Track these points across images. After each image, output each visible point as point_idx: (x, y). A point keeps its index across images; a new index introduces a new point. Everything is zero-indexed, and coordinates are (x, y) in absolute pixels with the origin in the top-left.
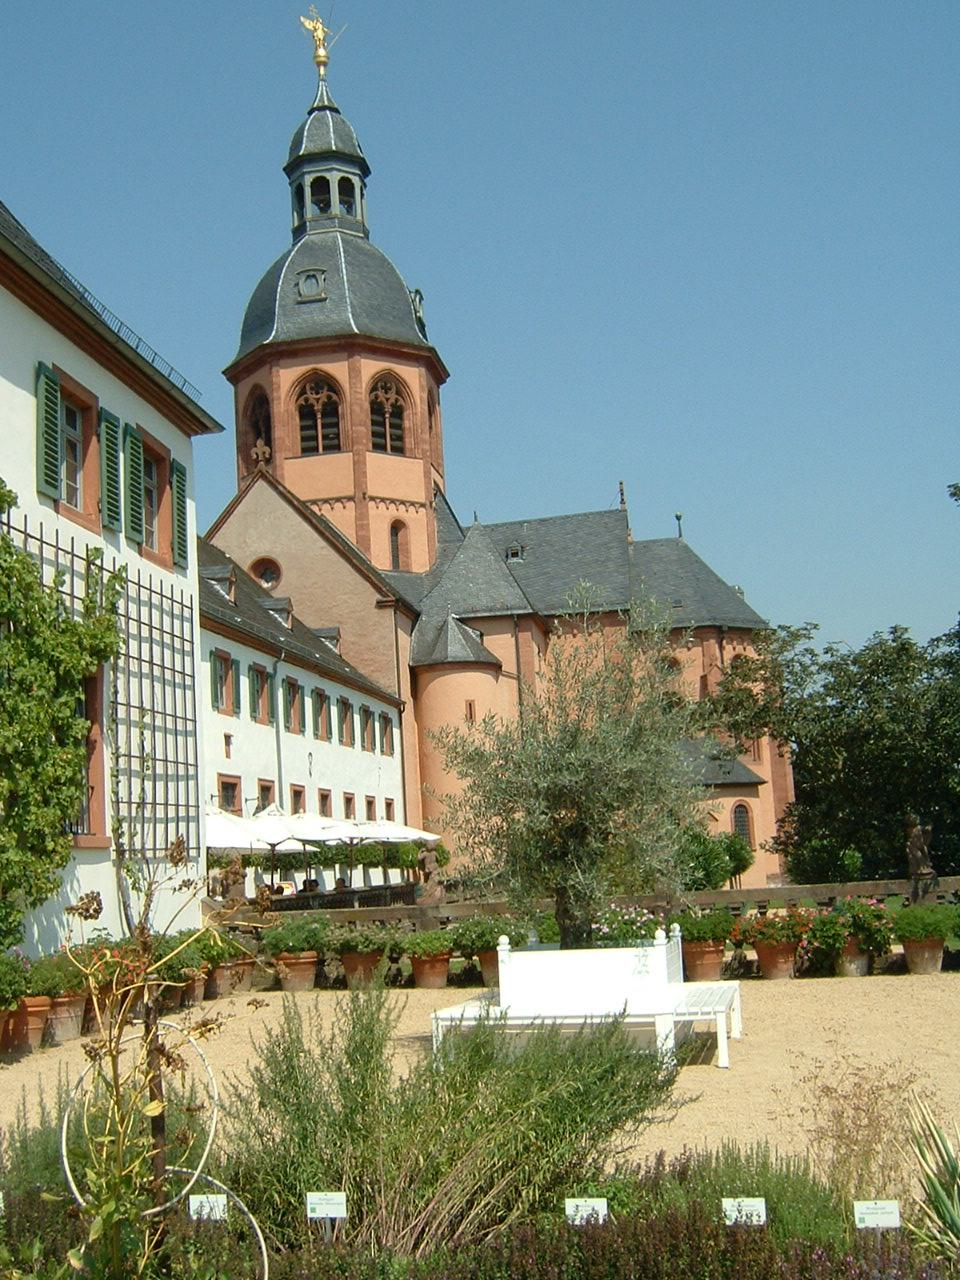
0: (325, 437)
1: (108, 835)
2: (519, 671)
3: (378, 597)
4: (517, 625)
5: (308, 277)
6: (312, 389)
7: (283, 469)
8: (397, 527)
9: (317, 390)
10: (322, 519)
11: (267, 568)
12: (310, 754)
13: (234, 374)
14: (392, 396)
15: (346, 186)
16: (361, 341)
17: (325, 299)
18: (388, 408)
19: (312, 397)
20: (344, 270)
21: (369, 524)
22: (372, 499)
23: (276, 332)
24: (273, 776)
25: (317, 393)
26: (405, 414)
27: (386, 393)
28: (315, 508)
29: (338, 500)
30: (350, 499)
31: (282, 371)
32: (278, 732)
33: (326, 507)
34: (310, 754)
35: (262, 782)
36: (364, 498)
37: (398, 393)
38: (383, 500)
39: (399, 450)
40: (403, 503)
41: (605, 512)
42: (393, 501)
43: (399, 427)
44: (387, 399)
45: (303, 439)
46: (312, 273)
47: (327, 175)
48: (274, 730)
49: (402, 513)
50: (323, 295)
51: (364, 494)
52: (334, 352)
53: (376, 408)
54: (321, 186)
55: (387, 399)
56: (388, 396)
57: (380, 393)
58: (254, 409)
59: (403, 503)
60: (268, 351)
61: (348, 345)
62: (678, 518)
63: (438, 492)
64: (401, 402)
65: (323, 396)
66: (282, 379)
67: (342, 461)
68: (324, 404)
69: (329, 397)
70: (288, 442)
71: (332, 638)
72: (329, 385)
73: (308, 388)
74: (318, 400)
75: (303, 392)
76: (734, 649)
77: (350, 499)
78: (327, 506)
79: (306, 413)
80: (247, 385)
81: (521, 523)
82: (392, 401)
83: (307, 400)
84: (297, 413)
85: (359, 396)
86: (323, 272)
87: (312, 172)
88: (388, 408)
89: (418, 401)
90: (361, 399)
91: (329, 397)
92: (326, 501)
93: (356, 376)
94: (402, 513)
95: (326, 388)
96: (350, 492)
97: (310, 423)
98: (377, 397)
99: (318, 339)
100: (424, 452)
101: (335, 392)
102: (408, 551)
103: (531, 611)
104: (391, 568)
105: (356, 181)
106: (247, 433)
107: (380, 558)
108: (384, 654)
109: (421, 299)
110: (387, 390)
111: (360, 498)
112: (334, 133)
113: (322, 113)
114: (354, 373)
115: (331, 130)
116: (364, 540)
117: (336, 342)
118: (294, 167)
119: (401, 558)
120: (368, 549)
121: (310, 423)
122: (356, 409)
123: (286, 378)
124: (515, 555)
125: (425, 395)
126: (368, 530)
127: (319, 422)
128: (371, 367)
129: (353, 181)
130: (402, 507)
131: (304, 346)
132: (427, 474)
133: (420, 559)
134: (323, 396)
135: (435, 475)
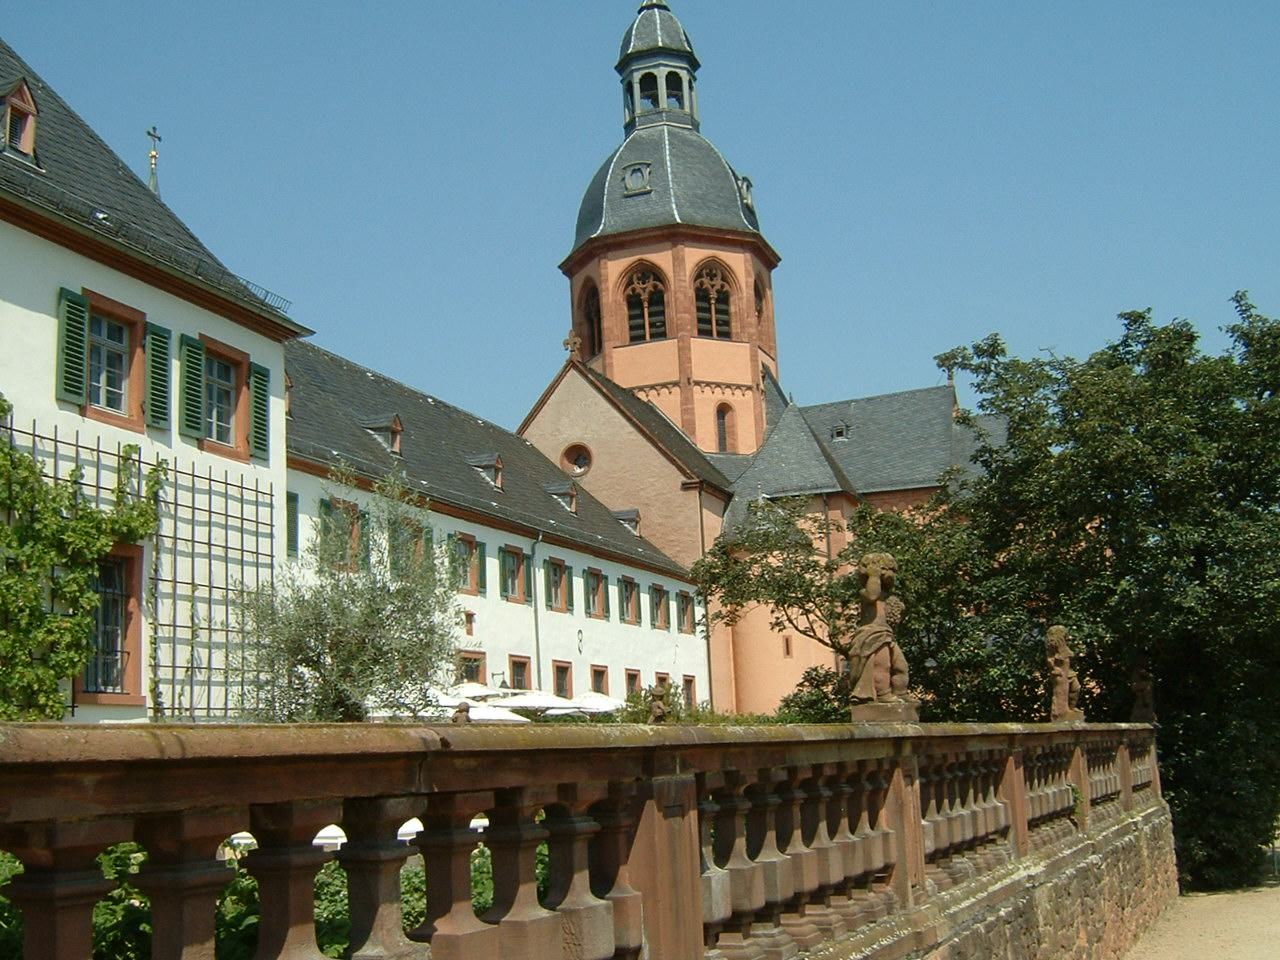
0: (652, 325)
1: (143, 695)
2: (829, 550)
3: (684, 479)
4: (826, 504)
5: (634, 171)
6: (639, 279)
7: (612, 358)
8: (723, 410)
9: (643, 279)
10: (650, 409)
11: (578, 454)
12: (580, 631)
13: (569, 268)
14: (718, 282)
15: (674, 81)
16: (683, 230)
17: (649, 192)
18: (713, 295)
19: (638, 286)
20: (668, 163)
21: (693, 409)
22: (697, 383)
23: (605, 225)
24: (526, 650)
25: (644, 283)
26: (731, 299)
27: (711, 280)
28: (642, 395)
29: (664, 385)
30: (675, 384)
31: (610, 263)
32: (536, 611)
33: (653, 392)
34: (580, 631)
35: (514, 659)
36: (689, 383)
37: (724, 279)
38: (708, 384)
39: (725, 335)
40: (728, 386)
41: (933, 389)
42: (718, 385)
43: (726, 312)
44: (713, 286)
45: (632, 328)
46: (637, 167)
47: (655, 71)
48: (533, 609)
49: (728, 396)
50: (648, 188)
51: (689, 379)
52: (661, 242)
53: (702, 295)
54: (649, 82)
55: (713, 286)
56: (713, 283)
57: (706, 281)
58: (587, 300)
59: (728, 386)
60: (596, 244)
61: (673, 235)
63: (766, 374)
64: (727, 288)
65: (649, 285)
66: (610, 270)
67: (668, 347)
68: (651, 294)
69: (655, 287)
70: (616, 332)
71: (630, 521)
72: (654, 274)
73: (635, 277)
74: (644, 289)
75: (630, 283)
77: (675, 384)
78: (654, 392)
79: (633, 302)
80: (580, 278)
81: (848, 403)
82: (718, 287)
83: (634, 290)
84: (625, 303)
85: (684, 284)
86: (648, 165)
87: (640, 69)
88: (713, 295)
89: (743, 285)
90: (686, 287)
91: (655, 287)
92: (652, 387)
93: (680, 265)
94: (728, 396)
95: (652, 277)
96: (675, 378)
97: (637, 312)
98: (702, 284)
99: (643, 230)
100: (750, 336)
101: (660, 281)
102: (734, 433)
103: (840, 489)
104: (718, 451)
105: (684, 75)
106: (581, 324)
107: (705, 440)
108: (689, 535)
109: (749, 186)
110: (712, 276)
111: (685, 383)
112: (661, 29)
113: (650, 11)
114: (678, 261)
115: (658, 27)
116: (690, 424)
117: (659, 233)
118: (624, 65)
119: (728, 441)
120: (693, 433)
121: (637, 312)
122: (681, 296)
123: (613, 270)
124: (840, 434)
125: (752, 280)
126: (693, 414)
127: (646, 310)
128: (694, 255)
129: (681, 75)
130: (728, 391)
131: (628, 238)
132: (754, 358)
133: (746, 441)
134: (649, 285)
135: (762, 357)
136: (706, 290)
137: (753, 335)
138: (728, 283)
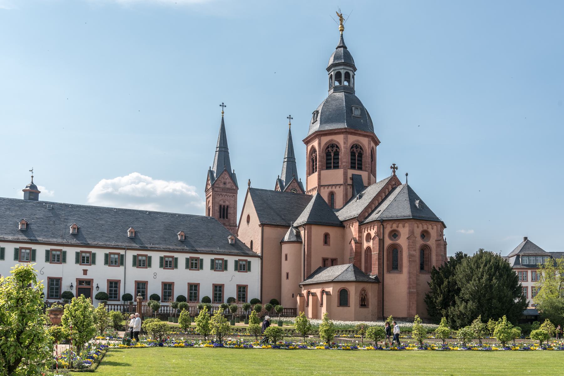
14: (335, 149)
18: (332, 154)
26: (340, 153)
39: (336, 167)
43: (338, 158)
44: (332, 150)
48: (124, 267)
49: (334, 189)
53: (328, 154)
62: (407, 175)
67: (316, 174)
74: (314, 155)
76: (391, 227)
88: (332, 154)
89: (343, 148)
94: (334, 189)
98: (329, 151)
117: (313, 136)
132: (345, 174)
135: (351, 172)
136: (330, 152)
137: (344, 165)
138: (338, 148)
